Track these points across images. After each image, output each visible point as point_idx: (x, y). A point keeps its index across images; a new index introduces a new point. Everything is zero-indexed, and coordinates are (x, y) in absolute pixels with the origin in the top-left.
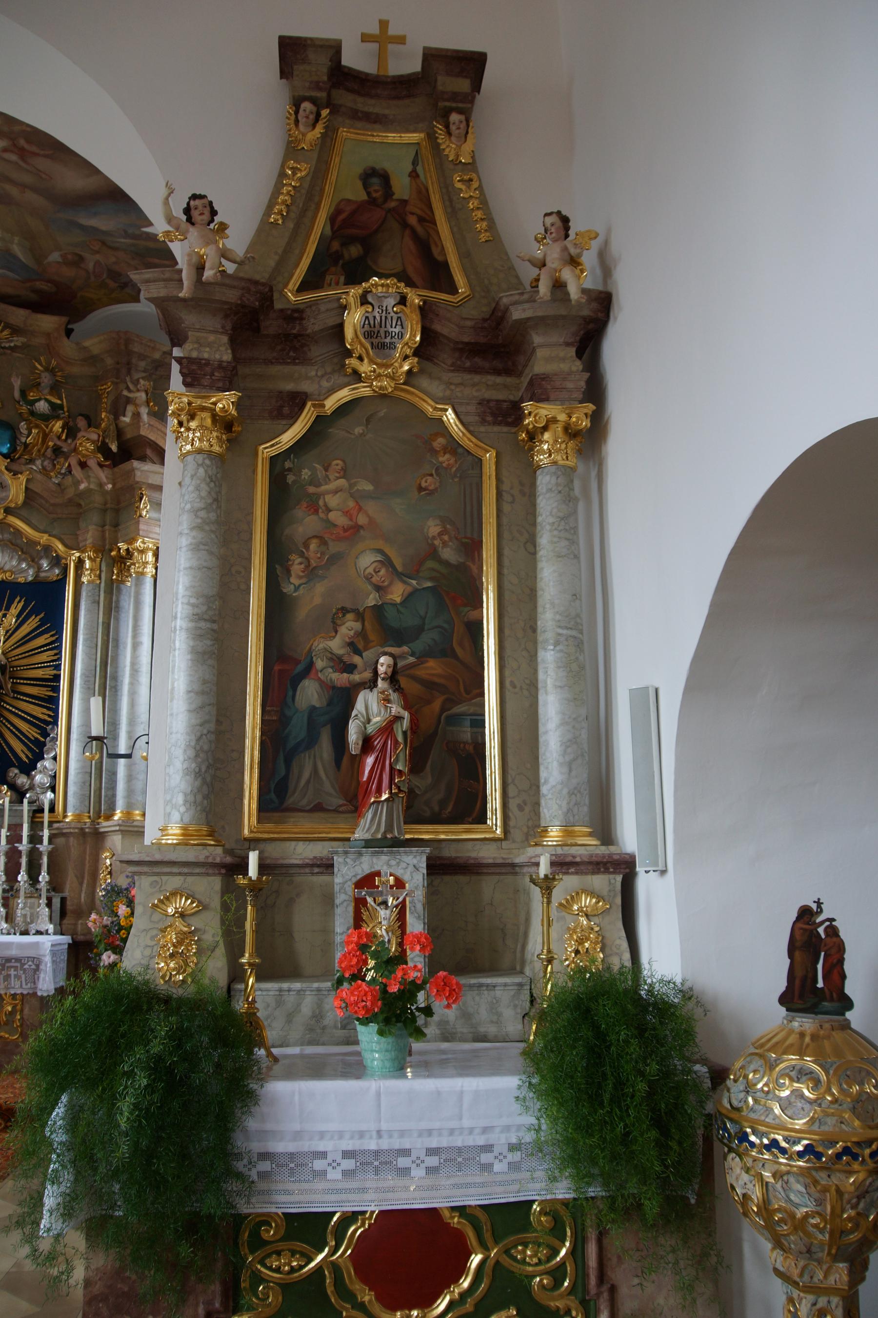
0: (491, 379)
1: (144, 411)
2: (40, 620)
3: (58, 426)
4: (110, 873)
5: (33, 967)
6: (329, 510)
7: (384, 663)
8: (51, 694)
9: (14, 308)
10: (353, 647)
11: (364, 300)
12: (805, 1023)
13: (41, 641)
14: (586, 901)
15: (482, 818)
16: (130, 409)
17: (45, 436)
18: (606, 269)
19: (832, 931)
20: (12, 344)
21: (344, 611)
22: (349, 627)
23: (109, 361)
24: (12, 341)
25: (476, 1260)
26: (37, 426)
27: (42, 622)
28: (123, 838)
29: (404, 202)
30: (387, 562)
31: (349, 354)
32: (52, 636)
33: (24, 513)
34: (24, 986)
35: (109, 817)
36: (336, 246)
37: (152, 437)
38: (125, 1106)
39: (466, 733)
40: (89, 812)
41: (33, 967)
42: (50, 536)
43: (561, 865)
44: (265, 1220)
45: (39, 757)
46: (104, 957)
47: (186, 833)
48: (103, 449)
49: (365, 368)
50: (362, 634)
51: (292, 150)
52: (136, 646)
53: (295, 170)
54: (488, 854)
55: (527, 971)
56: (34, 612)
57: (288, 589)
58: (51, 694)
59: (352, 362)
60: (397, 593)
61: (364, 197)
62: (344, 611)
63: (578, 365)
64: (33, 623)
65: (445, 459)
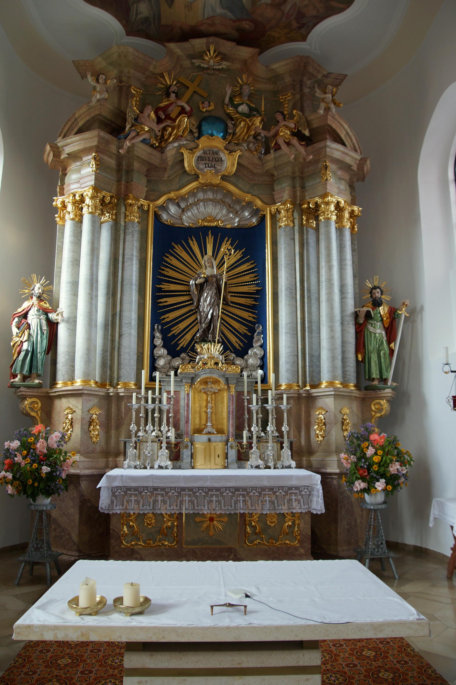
2: (243, 253)
3: (257, 121)
4: (325, 424)
5: (308, 493)
8: (254, 303)
9: (224, 41)
16: (323, 105)
17: (249, 128)
20: (220, 67)
23: (288, 80)
24: (220, 65)
27: (244, 255)
28: (335, 400)
32: (252, 264)
33: (233, 180)
34: (303, 507)
35: (315, 386)
40: (298, 383)
41: (308, 493)
46: (357, 483)
52: (330, 268)
58: (254, 303)
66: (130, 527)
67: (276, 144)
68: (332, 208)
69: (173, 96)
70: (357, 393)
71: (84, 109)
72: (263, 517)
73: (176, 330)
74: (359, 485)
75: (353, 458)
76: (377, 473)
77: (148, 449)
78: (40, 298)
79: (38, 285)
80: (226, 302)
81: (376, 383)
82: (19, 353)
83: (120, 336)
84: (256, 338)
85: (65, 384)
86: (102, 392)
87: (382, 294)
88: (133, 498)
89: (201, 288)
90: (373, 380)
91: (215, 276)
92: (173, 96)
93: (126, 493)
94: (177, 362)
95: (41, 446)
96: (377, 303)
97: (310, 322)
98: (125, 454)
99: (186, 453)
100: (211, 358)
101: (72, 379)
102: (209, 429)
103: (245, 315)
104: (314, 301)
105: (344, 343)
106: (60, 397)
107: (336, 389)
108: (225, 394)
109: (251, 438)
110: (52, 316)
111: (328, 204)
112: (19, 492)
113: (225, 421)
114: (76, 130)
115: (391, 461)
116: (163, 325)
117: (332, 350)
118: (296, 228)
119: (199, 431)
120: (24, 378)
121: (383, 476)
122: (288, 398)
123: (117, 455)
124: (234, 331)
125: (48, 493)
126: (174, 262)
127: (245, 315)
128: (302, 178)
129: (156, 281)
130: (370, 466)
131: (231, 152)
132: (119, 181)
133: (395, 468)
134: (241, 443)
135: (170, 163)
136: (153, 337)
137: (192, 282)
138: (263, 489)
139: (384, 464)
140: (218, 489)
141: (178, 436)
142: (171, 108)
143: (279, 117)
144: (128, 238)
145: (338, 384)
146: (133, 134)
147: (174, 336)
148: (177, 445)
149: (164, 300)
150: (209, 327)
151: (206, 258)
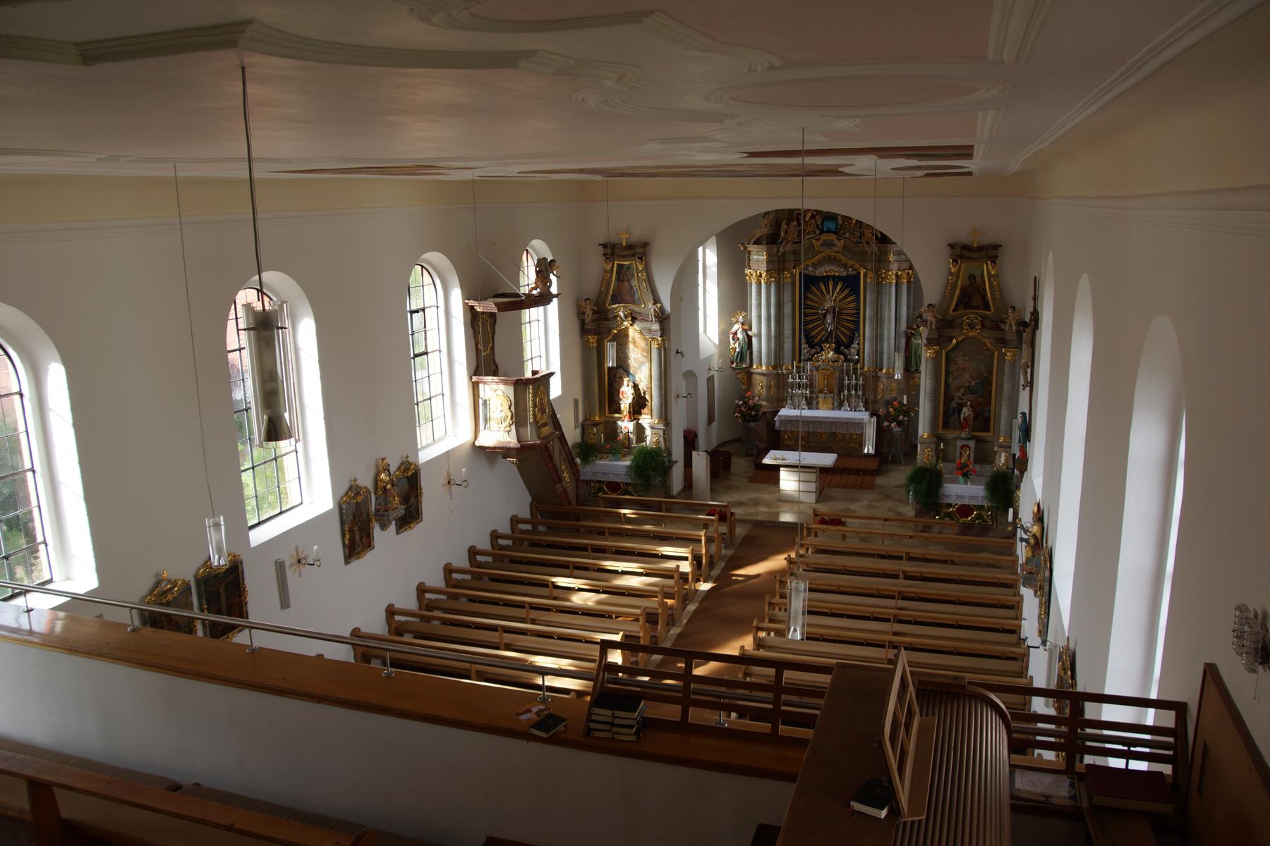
7: (969, 403)
11: (968, 319)
13: (850, 299)
21: (961, 387)
22: (962, 390)
25: (975, 513)
29: (979, 284)
30: (971, 376)
35: (881, 370)
38: (924, 488)
44: (942, 504)
47: (928, 436)
50: (965, 392)
51: (950, 274)
52: (890, 311)
54: (989, 439)
56: (847, 287)
59: (964, 331)
60: (973, 383)
61: (968, 283)
62: (961, 387)
64: (847, 291)
65: (986, 352)
66: (788, 436)
68: (894, 277)
72: (843, 434)
73: (813, 334)
77: (796, 400)
78: (743, 324)
79: (741, 317)
83: (784, 342)
85: (757, 368)
86: (775, 372)
89: (825, 315)
95: (751, 402)
98: (787, 400)
99: (814, 402)
102: (826, 391)
103: (850, 325)
110: (750, 333)
112: (743, 421)
114: (755, 239)
119: (821, 392)
120: (737, 364)
121: (895, 421)
123: (783, 400)
124: (844, 334)
125: (754, 422)
126: (811, 296)
127: (850, 325)
131: (839, 240)
133: (901, 418)
136: (800, 339)
138: (843, 423)
140: (824, 422)
141: (812, 392)
144: (786, 292)
147: (812, 337)
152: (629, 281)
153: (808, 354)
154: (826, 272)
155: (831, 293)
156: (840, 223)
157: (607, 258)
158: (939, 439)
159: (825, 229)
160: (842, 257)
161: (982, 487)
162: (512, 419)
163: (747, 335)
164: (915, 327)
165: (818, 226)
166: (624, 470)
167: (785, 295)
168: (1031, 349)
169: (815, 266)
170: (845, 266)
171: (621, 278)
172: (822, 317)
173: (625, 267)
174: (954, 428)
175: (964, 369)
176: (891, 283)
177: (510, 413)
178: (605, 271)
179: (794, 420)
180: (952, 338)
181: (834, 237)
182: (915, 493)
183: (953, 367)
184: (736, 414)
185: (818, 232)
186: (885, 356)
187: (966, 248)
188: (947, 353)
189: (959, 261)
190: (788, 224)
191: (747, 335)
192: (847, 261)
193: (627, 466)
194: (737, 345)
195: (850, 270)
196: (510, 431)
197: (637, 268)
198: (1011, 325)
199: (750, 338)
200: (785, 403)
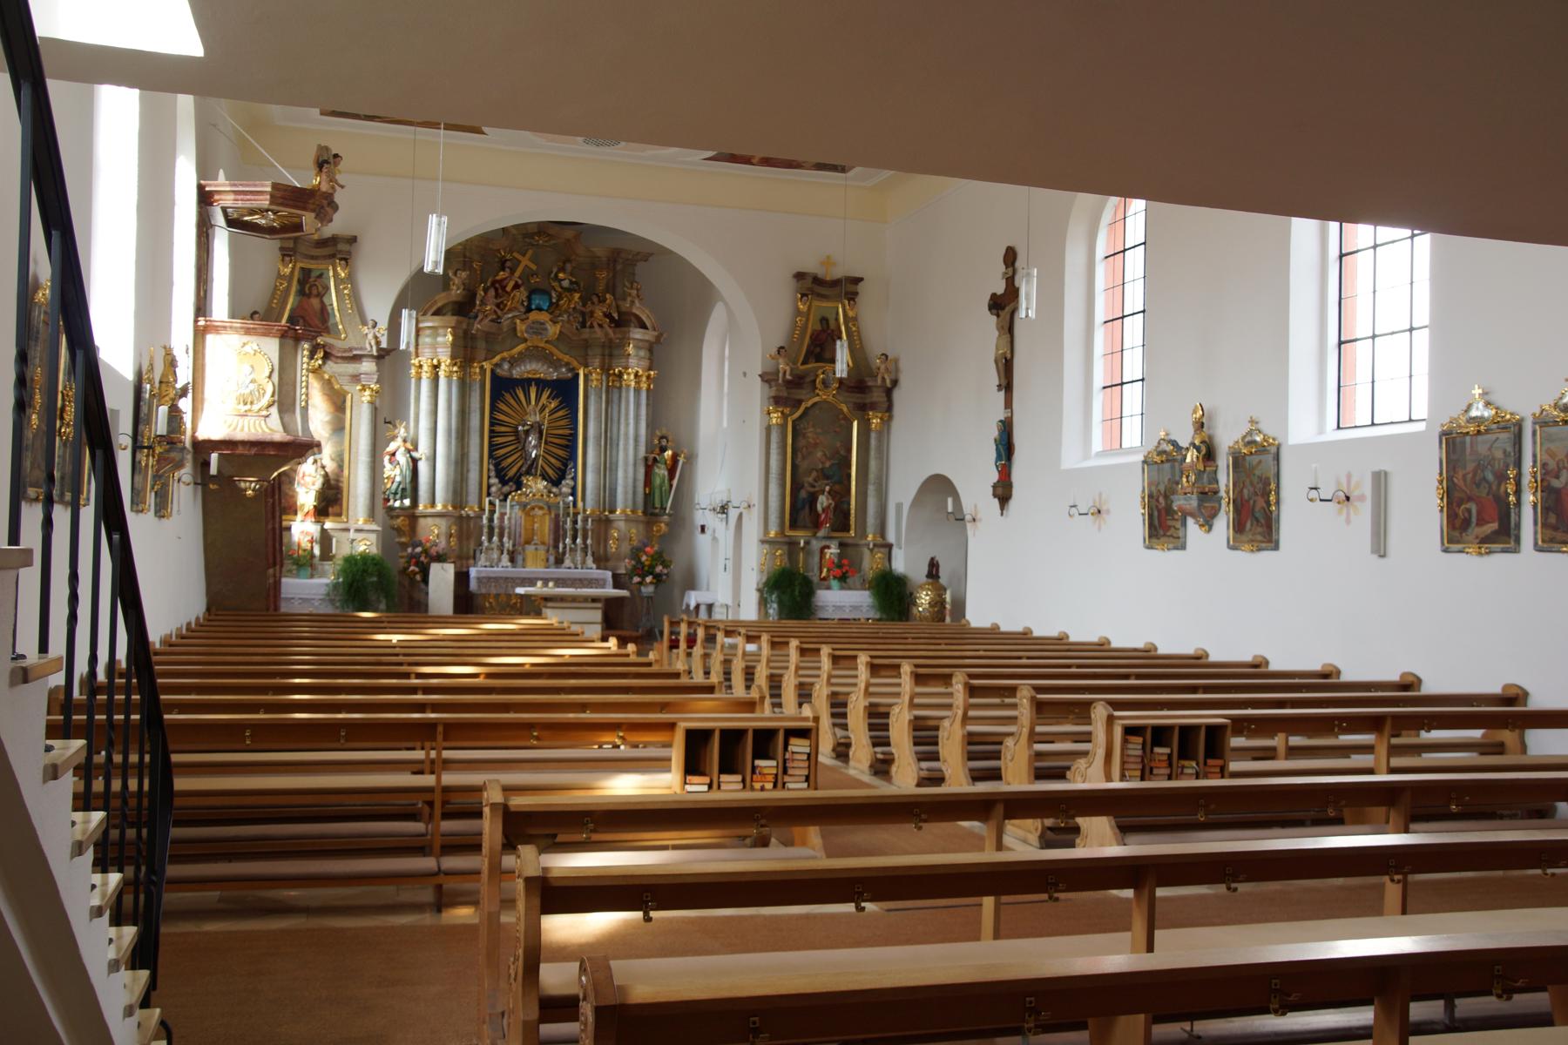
0: (858, 395)
1: (637, 301)
3: (577, 296)
6: (808, 437)
7: (827, 488)
10: (815, 481)
11: (823, 373)
12: (930, 581)
13: (561, 413)
14: (879, 555)
15: (848, 531)
16: (629, 299)
17: (570, 301)
18: (897, 370)
19: (937, 562)
22: (814, 474)
23: (604, 259)
26: (566, 296)
27: (561, 403)
29: (833, 331)
30: (825, 455)
31: (816, 388)
35: (612, 511)
36: (812, 348)
37: (638, 313)
39: (845, 506)
42: (571, 356)
43: (875, 545)
45: (562, 477)
47: (776, 534)
48: (608, 315)
49: (820, 393)
50: (818, 476)
51: (798, 312)
52: (627, 425)
53: (800, 320)
54: (850, 541)
55: (862, 573)
57: (797, 462)
59: (817, 391)
60: (828, 464)
62: (813, 469)
63: (885, 399)
65: (843, 422)
66: (490, 603)
67: (591, 324)
68: (632, 377)
69: (507, 270)
70: (643, 518)
71: (443, 294)
73: (505, 464)
74: (636, 579)
75: (633, 562)
76: (648, 572)
78: (405, 441)
80: (546, 443)
81: (657, 511)
82: (393, 483)
83: (468, 471)
84: (568, 472)
85: (426, 507)
87: (667, 441)
88: (493, 584)
89: (527, 433)
90: (656, 508)
91: (538, 423)
92: (507, 270)
93: (488, 581)
94: (506, 489)
96: (663, 450)
97: (611, 463)
98: (474, 558)
99: (519, 558)
100: (538, 490)
101: (433, 504)
102: (536, 542)
103: (560, 452)
104: (614, 446)
105: (635, 480)
106: (425, 516)
107: (626, 515)
108: (547, 517)
109: (565, 548)
110: (415, 454)
111: (629, 374)
113: (547, 536)
114: (434, 308)
115: (657, 565)
116: (496, 459)
117: (625, 487)
118: (604, 388)
121: (651, 574)
122: (592, 521)
123: (468, 558)
127: (560, 452)
128: (610, 347)
129: (492, 424)
130: (643, 568)
132: (466, 347)
133: (659, 569)
134: (558, 552)
135: (505, 330)
136: (489, 470)
137: (520, 428)
139: (652, 567)
141: (514, 545)
142: (505, 282)
143: (595, 299)
144: (473, 394)
145: (629, 512)
146: (480, 317)
147: (503, 469)
148: (513, 552)
149: (495, 439)
150: (533, 464)
151: (531, 407)
152: (320, 296)
153: (499, 493)
154: (529, 372)
155: (533, 402)
156: (554, 300)
157: (284, 255)
158: (792, 545)
159: (533, 307)
160: (555, 351)
161: (867, 593)
162: (273, 396)
163: (411, 457)
164: (657, 450)
165: (523, 301)
166: (323, 591)
167: (473, 400)
168: (1008, 335)
169: (513, 362)
170: (556, 364)
171: (307, 291)
172: (523, 436)
173: (314, 274)
174: (805, 527)
175: (816, 445)
176: (628, 386)
177: (270, 384)
178: (280, 276)
179: (501, 578)
180: (800, 402)
181: (544, 317)
182: (780, 603)
183: (802, 442)
184: (412, 568)
185: (523, 310)
186: (620, 490)
187: (817, 280)
188: (793, 422)
189: (810, 297)
190: (486, 290)
191: (411, 457)
192: (561, 356)
193: (327, 585)
194: (397, 471)
195: (564, 370)
196: (267, 416)
197: (336, 274)
198: (883, 379)
199: (415, 461)
200: (472, 561)
